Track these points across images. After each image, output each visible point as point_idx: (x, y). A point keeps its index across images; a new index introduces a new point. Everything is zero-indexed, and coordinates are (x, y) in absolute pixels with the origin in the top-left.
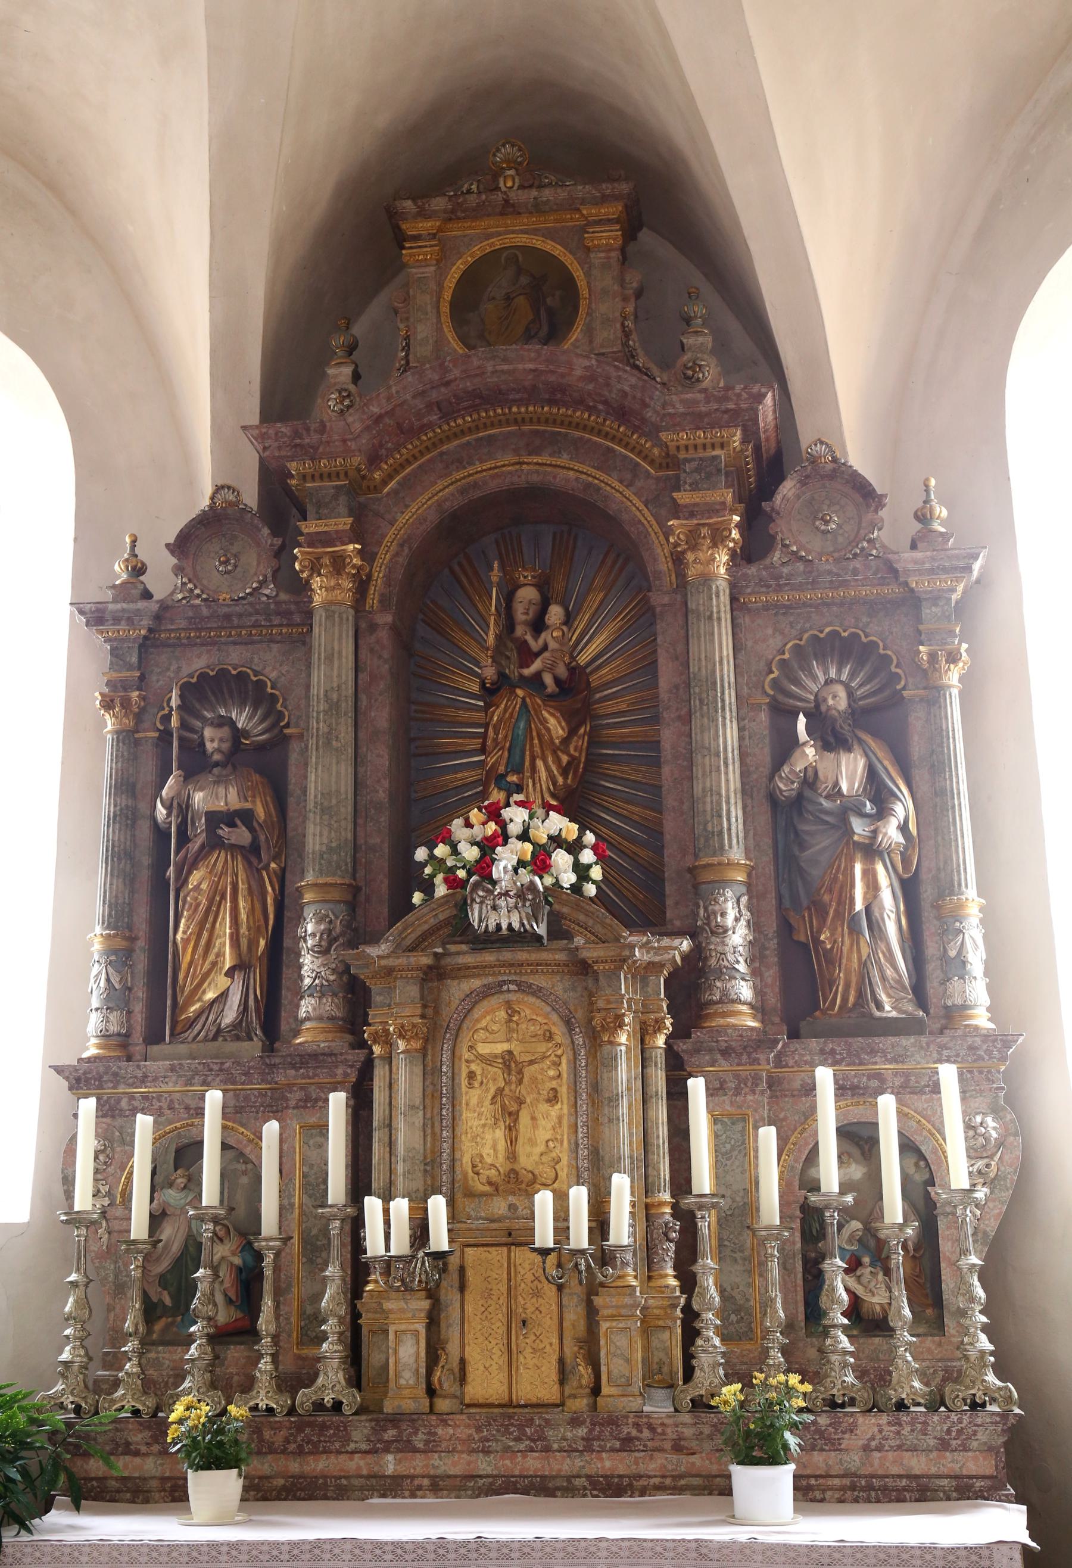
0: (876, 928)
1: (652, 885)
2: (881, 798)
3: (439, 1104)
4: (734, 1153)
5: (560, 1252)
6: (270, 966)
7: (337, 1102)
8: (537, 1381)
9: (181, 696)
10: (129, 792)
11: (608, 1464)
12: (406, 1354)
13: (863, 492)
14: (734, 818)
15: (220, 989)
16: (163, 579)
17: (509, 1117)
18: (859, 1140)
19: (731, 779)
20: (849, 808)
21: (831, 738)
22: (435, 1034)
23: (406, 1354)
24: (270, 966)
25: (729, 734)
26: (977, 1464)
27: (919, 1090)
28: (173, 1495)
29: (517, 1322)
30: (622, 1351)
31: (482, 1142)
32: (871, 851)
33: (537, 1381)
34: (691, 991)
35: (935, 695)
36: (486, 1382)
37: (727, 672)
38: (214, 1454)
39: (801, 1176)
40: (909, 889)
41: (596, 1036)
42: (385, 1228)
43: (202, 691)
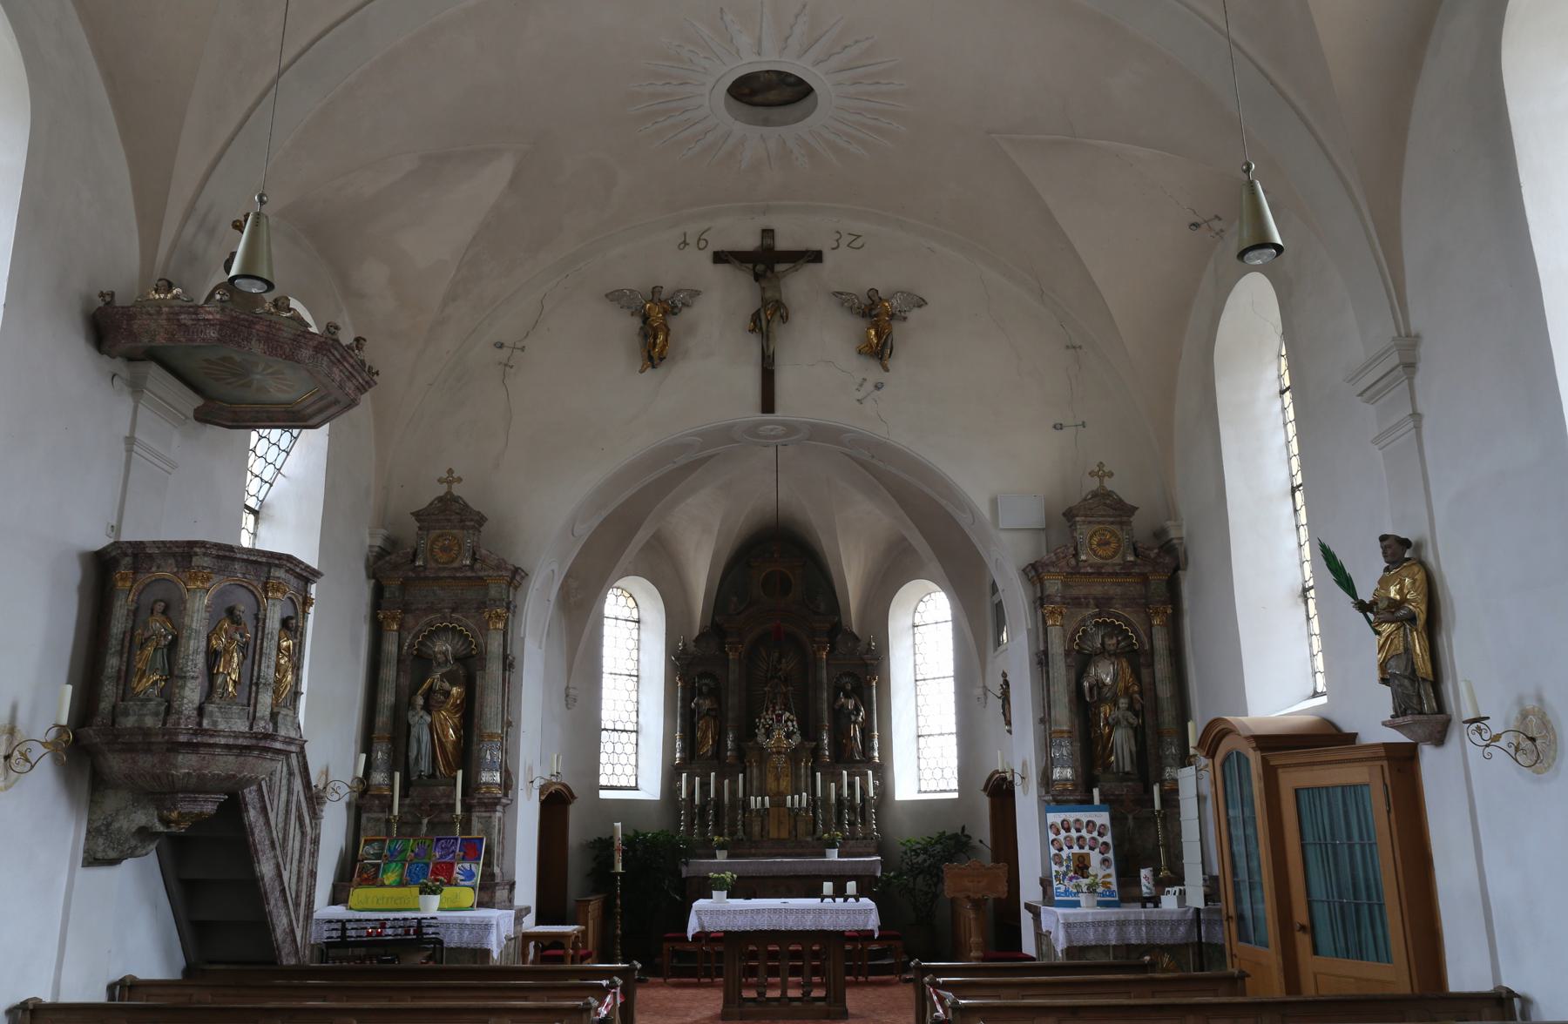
2: (858, 711)
4: (825, 788)
5: (791, 809)
8: (784, 835)
10: (686, 701)
11: (799, 851)
12: (756, 829)
13: (856, 639)
14: (826, 714)
15: (707, 748)
16: (692, 647)
17: (778, 779)
18: (851, 786)
19: (825, 706)
20: (851, 713)
21: (847, 696)
23: (756, 829)
27: (864, 776)
28: (715, 857)
29: (780, 822)
30: (801, 827)
31: (771, 784)
32: (855, 722)
33: (784, 835)
34: (816, 753)
36: (773, 834)
38: (722, 847)
40: (862, 731)
42: (755, 802)
43: (701, 676)
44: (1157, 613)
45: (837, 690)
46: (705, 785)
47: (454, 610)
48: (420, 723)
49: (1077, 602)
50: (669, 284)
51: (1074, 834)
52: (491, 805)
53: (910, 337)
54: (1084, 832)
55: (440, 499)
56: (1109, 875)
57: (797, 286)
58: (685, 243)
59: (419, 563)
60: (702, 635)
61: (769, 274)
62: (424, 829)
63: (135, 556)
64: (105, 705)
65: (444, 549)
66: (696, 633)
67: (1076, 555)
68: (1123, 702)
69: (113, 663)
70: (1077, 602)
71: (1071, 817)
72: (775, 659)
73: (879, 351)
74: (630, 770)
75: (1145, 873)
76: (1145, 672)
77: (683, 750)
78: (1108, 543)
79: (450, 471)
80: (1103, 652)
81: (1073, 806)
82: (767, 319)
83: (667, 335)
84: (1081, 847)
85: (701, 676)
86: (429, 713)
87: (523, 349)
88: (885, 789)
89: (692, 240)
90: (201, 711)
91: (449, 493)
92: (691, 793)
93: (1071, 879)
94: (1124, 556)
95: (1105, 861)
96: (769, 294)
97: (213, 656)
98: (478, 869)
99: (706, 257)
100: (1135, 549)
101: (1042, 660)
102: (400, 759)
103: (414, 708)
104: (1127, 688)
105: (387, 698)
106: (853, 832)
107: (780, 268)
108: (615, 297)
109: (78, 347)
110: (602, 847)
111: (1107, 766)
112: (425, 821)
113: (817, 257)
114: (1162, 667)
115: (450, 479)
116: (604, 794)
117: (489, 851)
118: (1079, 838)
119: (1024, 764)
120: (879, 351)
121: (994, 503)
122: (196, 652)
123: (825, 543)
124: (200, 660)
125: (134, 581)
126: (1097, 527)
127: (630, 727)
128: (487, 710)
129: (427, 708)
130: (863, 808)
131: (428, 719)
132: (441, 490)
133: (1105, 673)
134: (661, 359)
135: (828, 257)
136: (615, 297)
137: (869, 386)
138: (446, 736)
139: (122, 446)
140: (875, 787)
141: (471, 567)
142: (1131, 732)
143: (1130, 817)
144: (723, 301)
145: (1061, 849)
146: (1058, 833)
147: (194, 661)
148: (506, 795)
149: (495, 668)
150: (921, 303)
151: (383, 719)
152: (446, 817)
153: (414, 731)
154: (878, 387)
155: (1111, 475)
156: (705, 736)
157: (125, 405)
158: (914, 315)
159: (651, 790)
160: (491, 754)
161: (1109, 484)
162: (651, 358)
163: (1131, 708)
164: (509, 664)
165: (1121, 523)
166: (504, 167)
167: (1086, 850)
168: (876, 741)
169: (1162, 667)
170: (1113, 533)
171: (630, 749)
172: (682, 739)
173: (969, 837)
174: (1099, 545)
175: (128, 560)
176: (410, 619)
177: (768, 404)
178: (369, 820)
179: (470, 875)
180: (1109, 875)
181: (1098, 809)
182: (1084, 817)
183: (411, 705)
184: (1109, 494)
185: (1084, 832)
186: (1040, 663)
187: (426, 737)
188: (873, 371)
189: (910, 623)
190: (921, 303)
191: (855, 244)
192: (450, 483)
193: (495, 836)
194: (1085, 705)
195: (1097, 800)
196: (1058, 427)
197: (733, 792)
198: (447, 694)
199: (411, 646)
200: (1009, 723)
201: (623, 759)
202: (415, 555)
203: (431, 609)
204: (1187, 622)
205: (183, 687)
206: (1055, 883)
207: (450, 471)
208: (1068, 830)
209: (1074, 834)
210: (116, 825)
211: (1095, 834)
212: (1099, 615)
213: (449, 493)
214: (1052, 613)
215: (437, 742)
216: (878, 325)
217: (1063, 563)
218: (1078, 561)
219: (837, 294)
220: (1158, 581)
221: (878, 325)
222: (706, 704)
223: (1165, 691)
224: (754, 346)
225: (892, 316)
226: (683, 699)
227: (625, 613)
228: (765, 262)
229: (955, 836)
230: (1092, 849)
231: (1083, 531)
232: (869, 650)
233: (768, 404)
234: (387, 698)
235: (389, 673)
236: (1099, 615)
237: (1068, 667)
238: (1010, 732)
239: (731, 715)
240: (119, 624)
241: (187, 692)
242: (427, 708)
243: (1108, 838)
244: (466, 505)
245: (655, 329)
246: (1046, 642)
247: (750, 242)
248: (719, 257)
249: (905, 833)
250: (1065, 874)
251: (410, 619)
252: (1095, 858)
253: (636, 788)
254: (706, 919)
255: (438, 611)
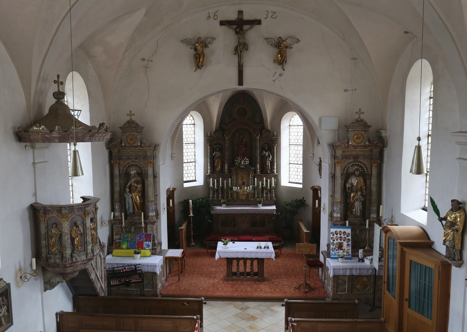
0: (268, 165)
1: (252, 163)
2: (269, 156)
3: (237, 179)
6: (223, 167)
7: (230, 179)
9: (213, 142)
10: (211, 153)
14: (258, 158)
19: (258, 155)
21: (266, 151)
22: (237, 174)
24: (223, 167)
25: (258, 151)
26: (273, 203)
34: (255, 171)
35: (274, 148)
37: (258, 146)
38: (224, 203)
39: (263, 184)
40: (271, 163)
41: (249, 175)
42: (235, 189)
43: (216, 144)
44: (374, 162)
45: (263, 149)
46: (218, 181)
47: (136, 159)
48: (128, 197)
49: (347, 157)
50: (203, 34)
51: (339, 236)
52: (153, 223)
53: (293, 55)
54: (342, 235)
55: (128, 122)
56: (349, 249)
57: (252, 35)
58: (209, 17)
59: (123, 144)
60: (216, 130)
61: (241, 32)
62: (133, 230)
63: (44, 210)
64: (44, 255)
65: (131, 139)
66: (214, 130)
67: (348, 142)
68: (359, 193)
69: (43, 242)
70: (347, 157)
71: (338, 230)
72: (242, 135)
73: (281, 61)
74: (193, 175)
75: (361, 251)
76: (368, 181)
77: (210, 169)
78: (359, 138)
79: (131, 111)
80: (353, 174)
81: (339, 226)
82: (241, 49)
83: (204, 57)
84: (341, 240)
85: (216, 144)
86: (131, 193)
87: (152, 61)
88: (278, 182)
89: (212, 16)
90: (72, 256)
91: (131, 119)
92: (213, 184)
93: (336, 250)
94: (365, 143)
95: (348, 245)
96: (241, 41)
97: (72, 239)
98: (150, 244)
99: (217, 23)
100: (369, 140)
101: (333, 177)
102: (123, 208)
103: (126, 192)
104: (361, 187)
105: (117, 189)
106: (267, 197)
107: (246, 27)
108: (185, 41)
109: (14, 144)
110: (186, 203)
111: (352, 212)
112: (133, 228)
113: (258, 22)
114: (374, 181)
115: (131, 114)
116: (186, 185)
117: (154, 237)
118: (340, 237)
119: (324, 204)
120: (281, 61)
121: (320, 119)
122: (68, 239)
123: (259, 100)
124: (69, 241)
125: (45, 217)
126: (356, 132)
127: (193, 160)
128: (149, 193)
129: (130, 192)
130: (270, 190)
131: (131, 195)
132: (128, 118)
133: (354, 181)
134: (202, 66)
135: (263, 22)
136: (185, 41)
137: (277, 75)
138: (137, 201)
139: (32, 167)
140: (274, 182)
141: (141, 146)
142: (361, 203)
143: (358, 230)
144: (224, 40)
145: (334, 241)
146: (333, 235)
147: (67, 239)
148: (157, 218)
149: (151, 179)
150: (298, 41)
151: (116, 196)
152: (139, 226)
153: (127, 200)
154: (281, 75)
155: (363, 113)
156: (218, 164)
157: (31, 151)
158: (295, 46)
159: (200, 182)
160: (151, 207)
161: (362, 117)
162: (198, 66)
163: (362, 195)
164: (155, 176)
165: (365, 131)
166: (143, 11)
167: (342, 241)
168: (275, 166)
169: (374, 181)
170: (362, 135)
171: (193, 168)
172: (210, 166)
173: (305, 201)
174: (356, 139)
175: (42, 211)
176: (122, 162)
177: (241, 82)
178: (115, 227)
179: (148, 246)
180: (349, 249)
181: (347, 228)
182: (343, 230)
183: (125, 191)
184: (362, 121)
185: (342, 235)
186: (332, 177)
187: (131, 202)
188: (279, 69)
189: (288, 125)
190: (298, 41)
191: (274, 16)
192: (131, 116)
193: (155, 232)
194: (346, 192)
195: (347, 225)
196: (346, 91)
197: (227, 184)
198: (137, 188)
199: (123, 170)
200: (321, 175)
201: (191, 171)
202: (121, 141)
203: (128, 158)
204: (385, 166)
205: (66, 250)
206: (331, 251)
207: (131, 111)
208: (337, 234)
209: (339, 236)
210: (51, 281)
211: (346, 236)
212: (354, 162)
213: (131, 119)
214: (338, 162)
215: (134, 203)
216: (281, 50)
217: (343, 145)
218: (348, 145)
219: (267, 39)
220: (376, 151)
221: (281, 50)
222: (218, 154)
223: (374, 189)
224: (236, 59)
225: (286, 47)
226: (210, 153)
227: (189, 122)
228: (239, 25)
229: (300, 200)
230: (344, 241)
231: (351, 134)
232: (273, 135)
233: (241, 82)
234: (117, 189)
235: (117, 181)
236: (354, 162)
237: (342, 179)
238: (321, 177)
239: (226, 158)
240: (43, 230)
241: (67, 252)
242: (130, 192)
243: (350, 238)
244: (137, 124)
245: (199, 52)
246: (335, 171)
247: (233, 16)
248: (222, 23)
249: (285, 198)
250: (335, 249)
251: (122, 162)
252: (345, 244)
253: (195, 181)
254: (221, 254)
255: (131, 159)
